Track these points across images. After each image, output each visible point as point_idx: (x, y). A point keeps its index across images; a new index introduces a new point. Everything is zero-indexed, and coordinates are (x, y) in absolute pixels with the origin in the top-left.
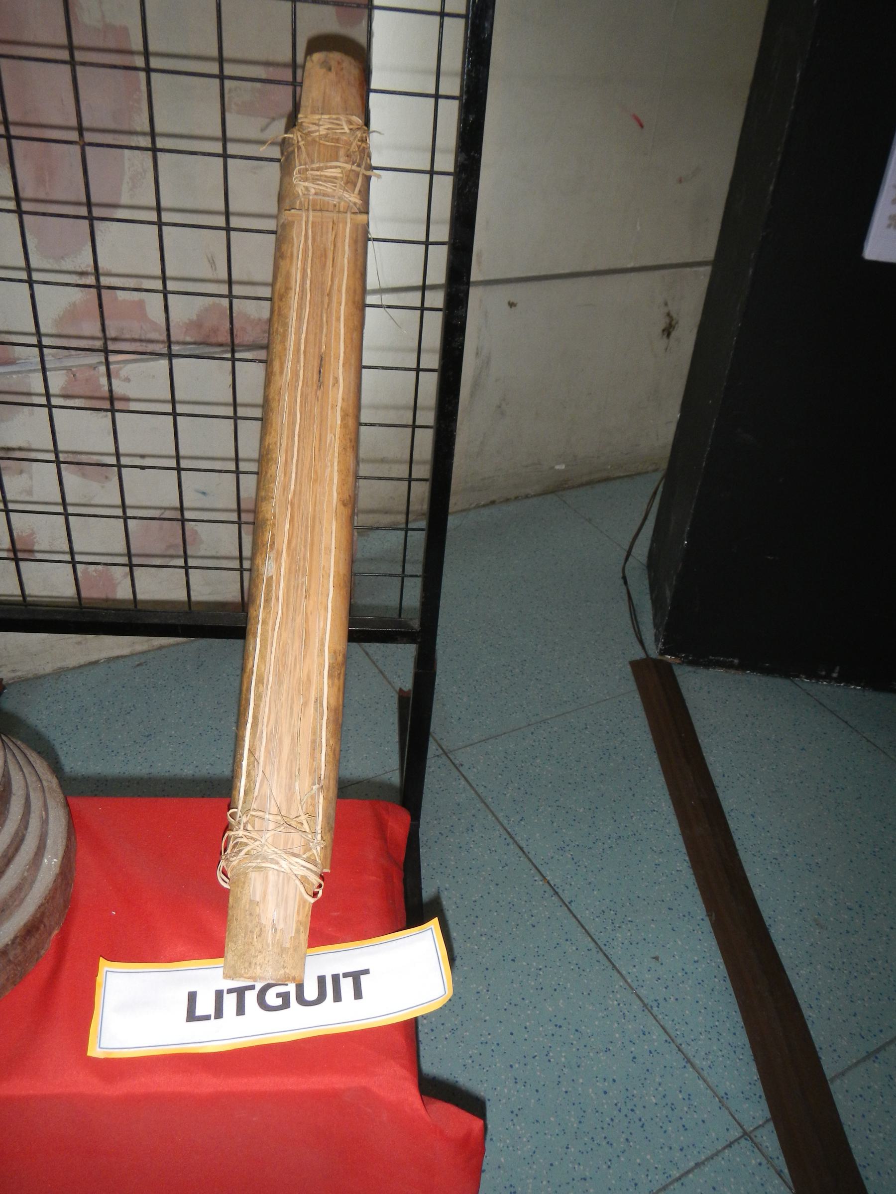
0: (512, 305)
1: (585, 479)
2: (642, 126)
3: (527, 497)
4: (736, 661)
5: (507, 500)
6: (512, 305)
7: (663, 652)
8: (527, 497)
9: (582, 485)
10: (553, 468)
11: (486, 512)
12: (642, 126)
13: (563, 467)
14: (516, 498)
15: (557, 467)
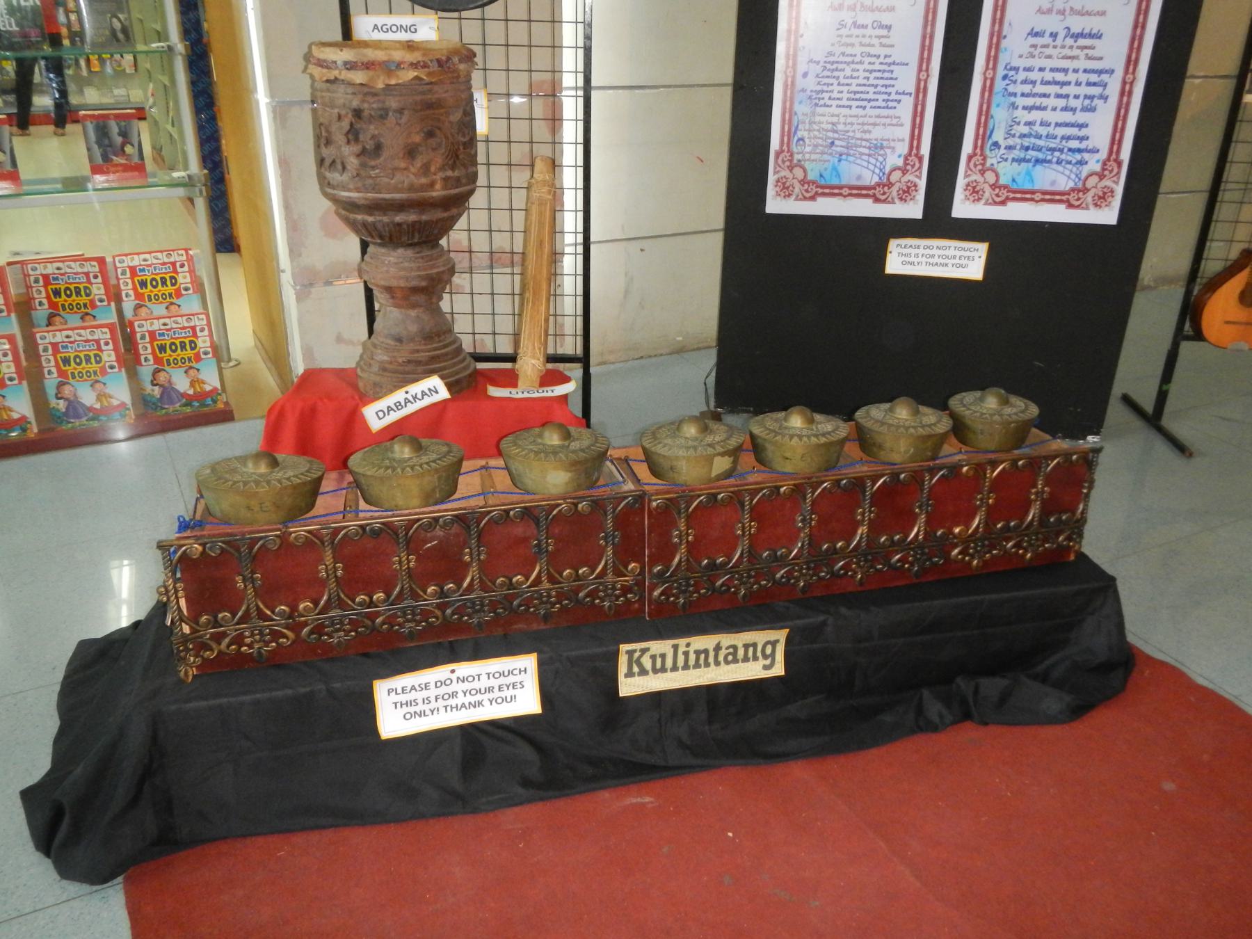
0: (642, 250)
1: (695, 347)
2: (702, 161)
3: (661, 355)
4: (752, 409)
5: (650, 356)
6: (642, 250)
7: (716, 407)
8: (661, 355)
9: (694, 350)
10: (675, 339)
11: (638, 361)
12: (702, 161)
13: (680, 339)
14: (655, 356)
15: (678, 339)
